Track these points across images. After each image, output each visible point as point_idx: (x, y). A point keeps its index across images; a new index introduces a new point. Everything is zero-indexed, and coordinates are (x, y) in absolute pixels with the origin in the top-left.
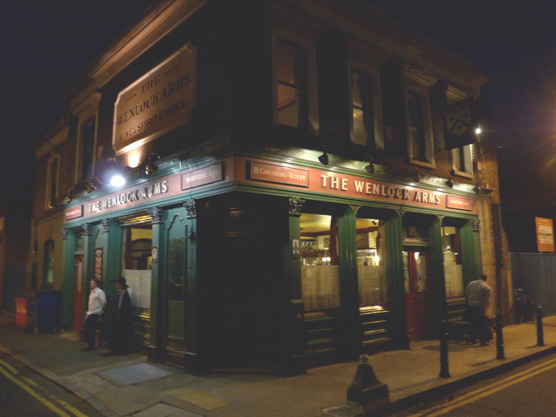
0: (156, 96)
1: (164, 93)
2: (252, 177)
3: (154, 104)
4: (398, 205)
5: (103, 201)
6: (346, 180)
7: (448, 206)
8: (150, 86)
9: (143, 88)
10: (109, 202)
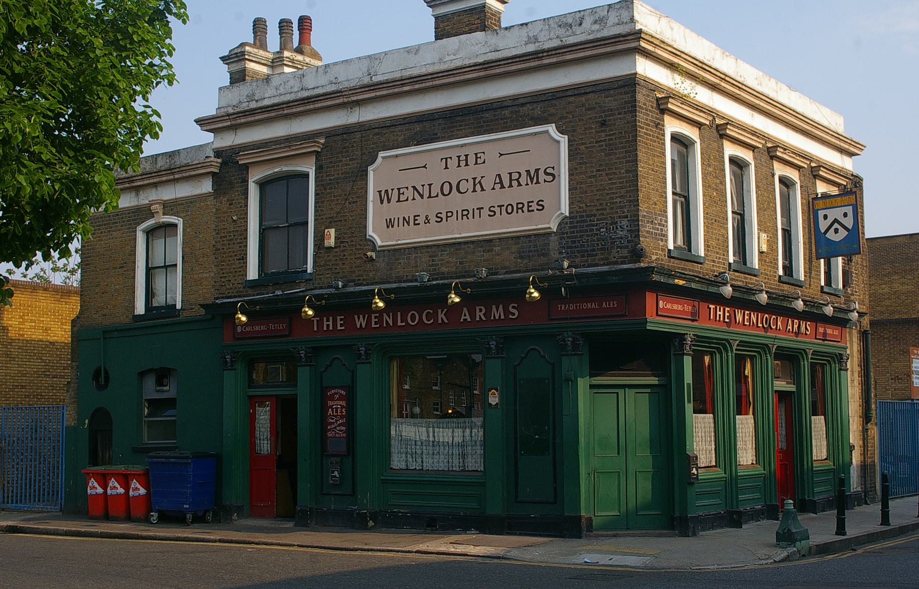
0: (477, 182)
1: (498, 181)
2: (659, 313)
3: (474, 191)
4: (772, 338)
5: (356, 317)
6: (729, 309)
7: (817, 337)
8: (463, 163)
9: (444, 160)
10: (373, 320)
